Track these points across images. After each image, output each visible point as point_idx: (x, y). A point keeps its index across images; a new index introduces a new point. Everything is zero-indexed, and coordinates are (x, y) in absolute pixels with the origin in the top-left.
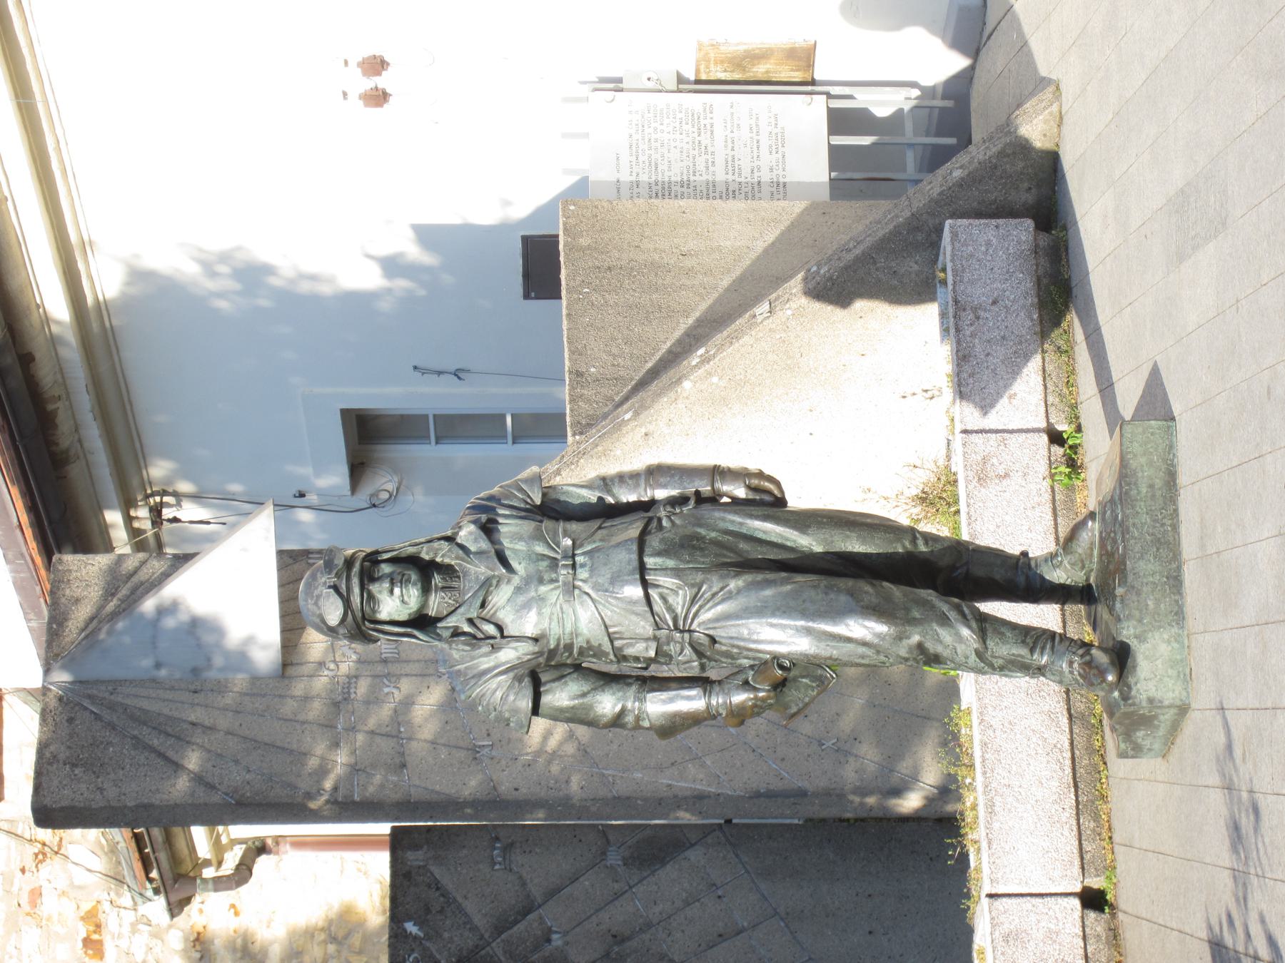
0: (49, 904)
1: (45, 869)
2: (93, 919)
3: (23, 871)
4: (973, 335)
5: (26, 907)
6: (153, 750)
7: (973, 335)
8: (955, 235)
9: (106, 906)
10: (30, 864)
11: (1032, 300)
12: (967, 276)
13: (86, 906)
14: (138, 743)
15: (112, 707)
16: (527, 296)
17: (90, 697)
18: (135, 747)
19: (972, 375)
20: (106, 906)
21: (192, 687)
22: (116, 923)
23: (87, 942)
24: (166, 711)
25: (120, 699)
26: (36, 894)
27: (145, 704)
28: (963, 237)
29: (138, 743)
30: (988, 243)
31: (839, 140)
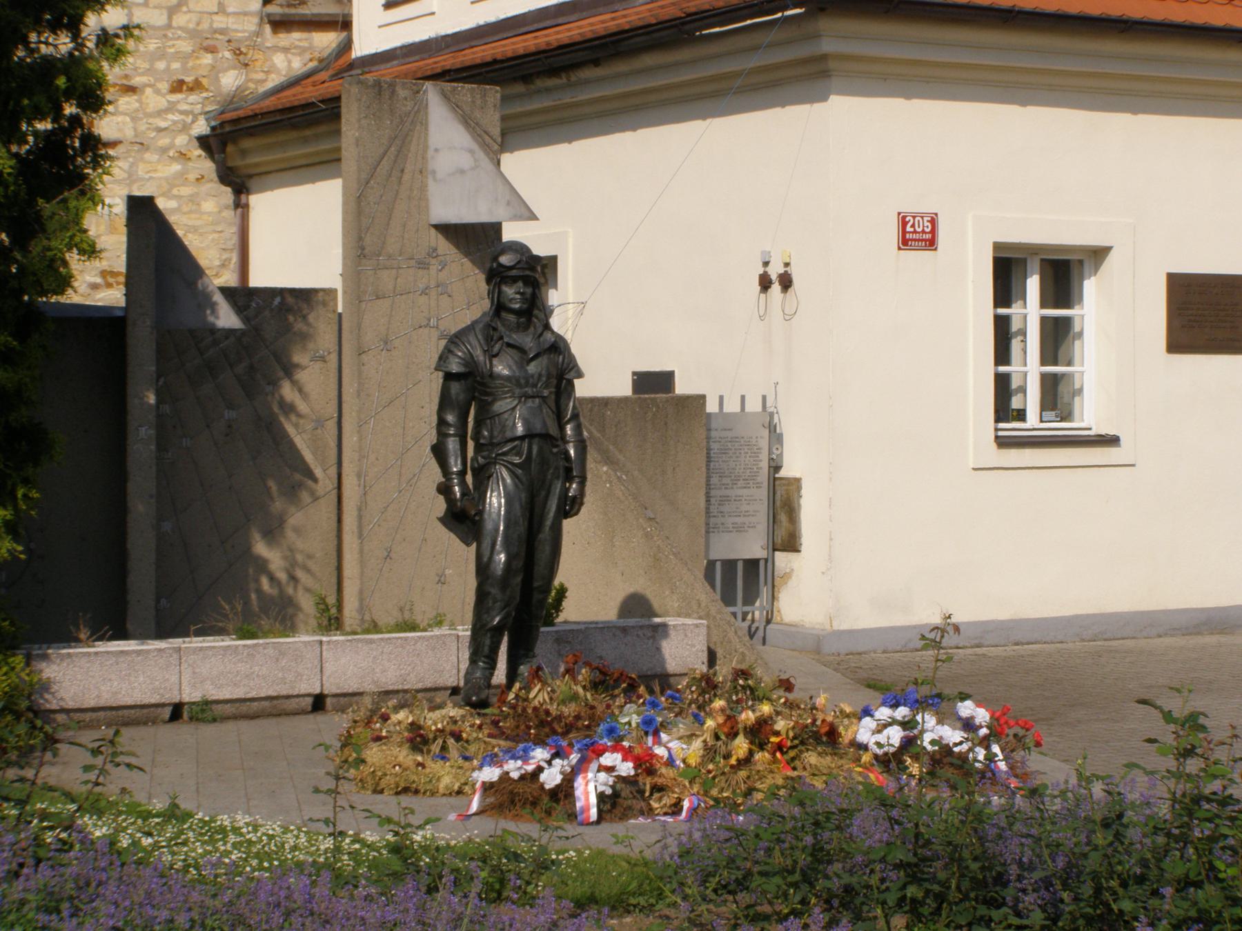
0: (207, 59)
1: (228, 54)
2: (196, 86)
3: (229, 41)
4: (638, 636)
5: (205, 43)
7: (638, 636)
8: (697, 626)
9: (205, 95)
10: (234, 45)
13: (205, 82)
16: (634, 374)
19: (614, 635)
20: (205, 95)
22: (192, 101)
26: (212, 50)
28: (697, 631)
29: (392, 139)
30: (693, 646)
31: (740, 566)
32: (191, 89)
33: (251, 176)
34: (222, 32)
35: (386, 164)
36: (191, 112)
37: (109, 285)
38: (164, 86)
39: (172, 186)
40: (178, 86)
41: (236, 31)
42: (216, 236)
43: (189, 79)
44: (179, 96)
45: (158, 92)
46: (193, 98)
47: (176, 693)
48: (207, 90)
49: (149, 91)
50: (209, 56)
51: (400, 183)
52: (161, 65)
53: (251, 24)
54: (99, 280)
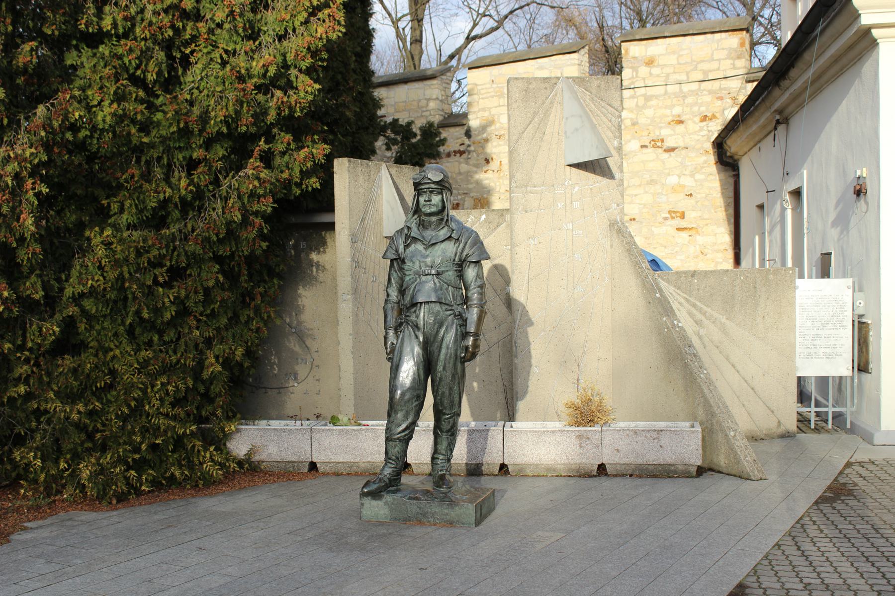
1: (729, 101)
2: (714, 117)
6: (533, 119)
10: (731, 95)
11: (662, 462)
12: (673, 436)
13: (718, 115)
14: (535, 114)
15: (552, 103)
17: (556, 94)
18: (534, 113)
23: (706, 116)
26: (721, 98)
27: (553, 115)
30: (689, 446)
31: (813, 380)
34: (725, 89)
37: (673, 218)
38: (697, 119)
39: (702, 168)
40: (704, 118)
43: (709, 115)
44: (704, 123)
45: (694, 122)
47: (309, 455)
49: (690, 122)
50: (720, 102)
51: (542, 139)
52: (696, 109)
54: (668, 215)
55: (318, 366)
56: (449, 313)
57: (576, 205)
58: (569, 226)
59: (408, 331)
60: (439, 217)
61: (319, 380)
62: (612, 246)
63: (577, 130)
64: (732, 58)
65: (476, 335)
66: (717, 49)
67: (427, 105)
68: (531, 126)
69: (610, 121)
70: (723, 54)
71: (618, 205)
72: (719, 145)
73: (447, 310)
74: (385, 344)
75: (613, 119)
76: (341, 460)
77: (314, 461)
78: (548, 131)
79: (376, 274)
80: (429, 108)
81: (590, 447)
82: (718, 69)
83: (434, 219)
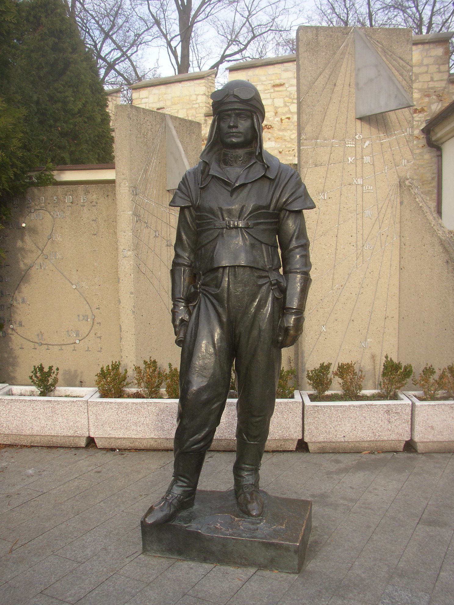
0: (426, 100)
1: (434, 97)
2: (422, 111)
5: (426, 93)
10: (436, 93)
13: (425, 109)
15: (343, 53)
21: (351, 84)
24: (341, 74)
25: (346, 56)
26: (428, 96)
27: (344, 66)
32: (420, 112)
33: (442, 143)
34: (432, 88)
35: (321, 81)
36: (420, 121)
41: (438, 87)
42: (430, 168)
43: (419, 108)
46: (420, 115)
48: (426, 112)
50: (427, 98)
53: (443, 84)
55: (100, 323)
56: (261, 282)
57: (367, 159)
58: (360, 181)
59: (205, 305)
60: (246, 150)
61: (100, 337)
62: (401, 203)
63: (371, 80)
64: (438, 64)
65: (300, 311)
66: (426, 57)
67: (197, 99)
68: (322, 76)
69: (401, 75)
70: (431, 60)
71: (408, 162)
72: (428, 131)
73: (260, 277)
74: (174, 321)
75: (405, 73)
76: (121, 436)
77: (92, 435)
78: (339, 82)
79: (159, 228)
80: (198, 101)
81: (398, 422)
82: (427, 72)
83: (240, 152)
